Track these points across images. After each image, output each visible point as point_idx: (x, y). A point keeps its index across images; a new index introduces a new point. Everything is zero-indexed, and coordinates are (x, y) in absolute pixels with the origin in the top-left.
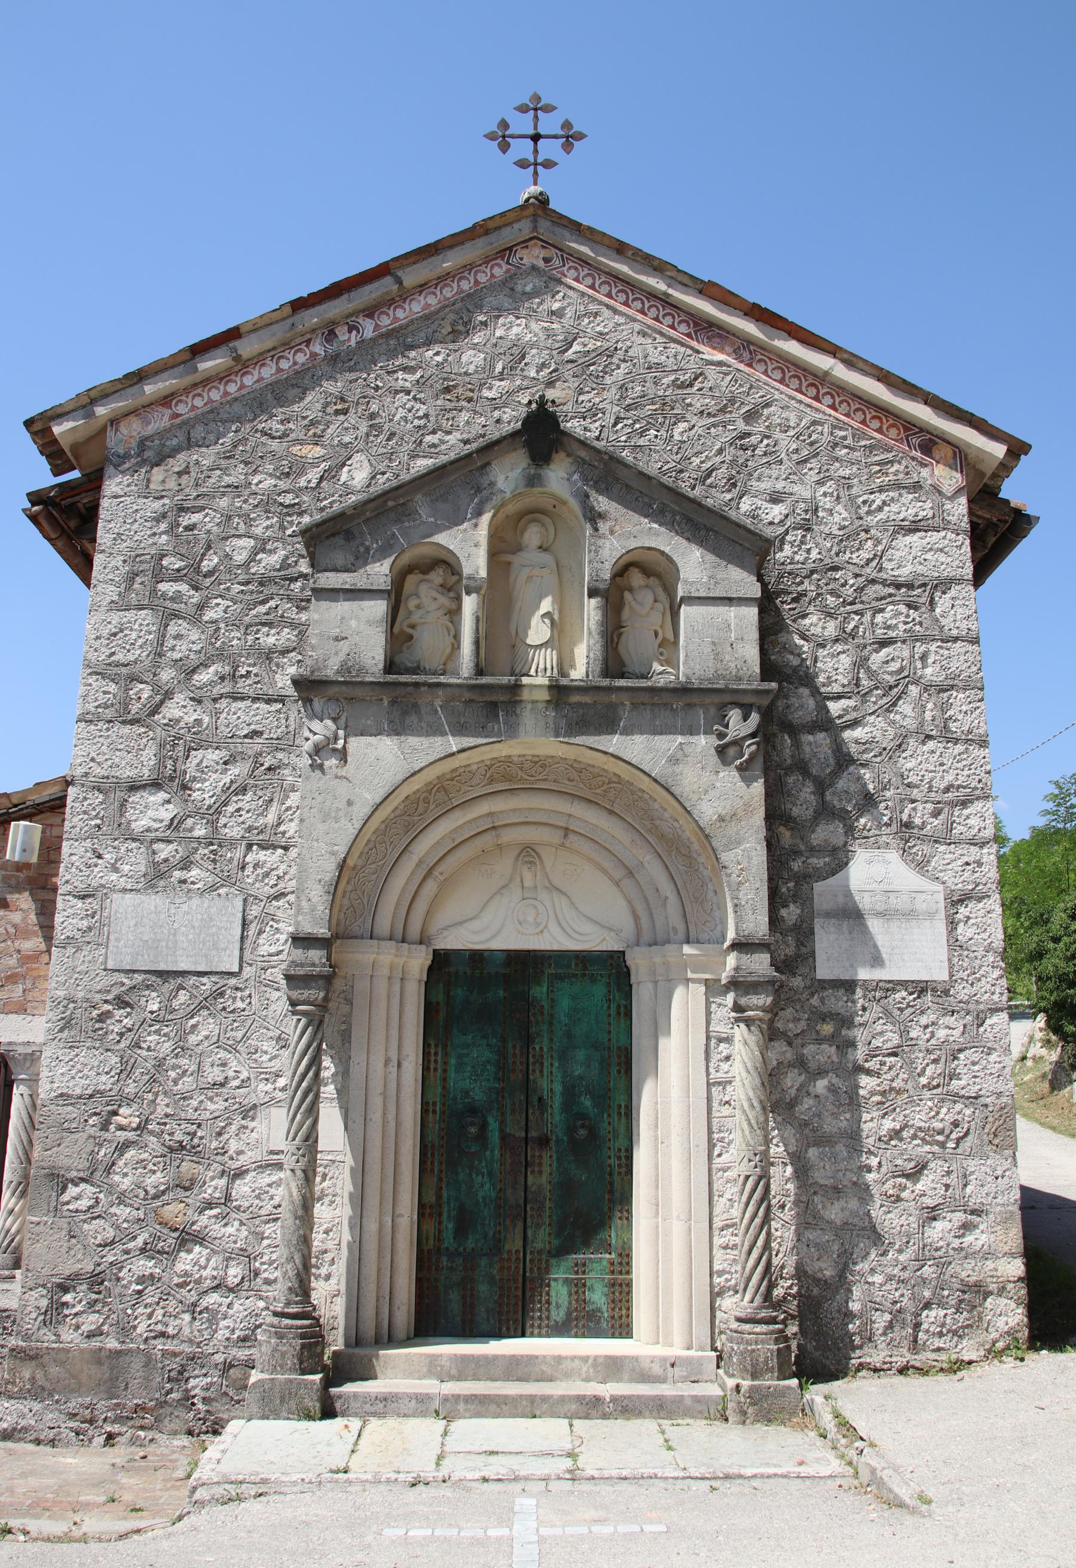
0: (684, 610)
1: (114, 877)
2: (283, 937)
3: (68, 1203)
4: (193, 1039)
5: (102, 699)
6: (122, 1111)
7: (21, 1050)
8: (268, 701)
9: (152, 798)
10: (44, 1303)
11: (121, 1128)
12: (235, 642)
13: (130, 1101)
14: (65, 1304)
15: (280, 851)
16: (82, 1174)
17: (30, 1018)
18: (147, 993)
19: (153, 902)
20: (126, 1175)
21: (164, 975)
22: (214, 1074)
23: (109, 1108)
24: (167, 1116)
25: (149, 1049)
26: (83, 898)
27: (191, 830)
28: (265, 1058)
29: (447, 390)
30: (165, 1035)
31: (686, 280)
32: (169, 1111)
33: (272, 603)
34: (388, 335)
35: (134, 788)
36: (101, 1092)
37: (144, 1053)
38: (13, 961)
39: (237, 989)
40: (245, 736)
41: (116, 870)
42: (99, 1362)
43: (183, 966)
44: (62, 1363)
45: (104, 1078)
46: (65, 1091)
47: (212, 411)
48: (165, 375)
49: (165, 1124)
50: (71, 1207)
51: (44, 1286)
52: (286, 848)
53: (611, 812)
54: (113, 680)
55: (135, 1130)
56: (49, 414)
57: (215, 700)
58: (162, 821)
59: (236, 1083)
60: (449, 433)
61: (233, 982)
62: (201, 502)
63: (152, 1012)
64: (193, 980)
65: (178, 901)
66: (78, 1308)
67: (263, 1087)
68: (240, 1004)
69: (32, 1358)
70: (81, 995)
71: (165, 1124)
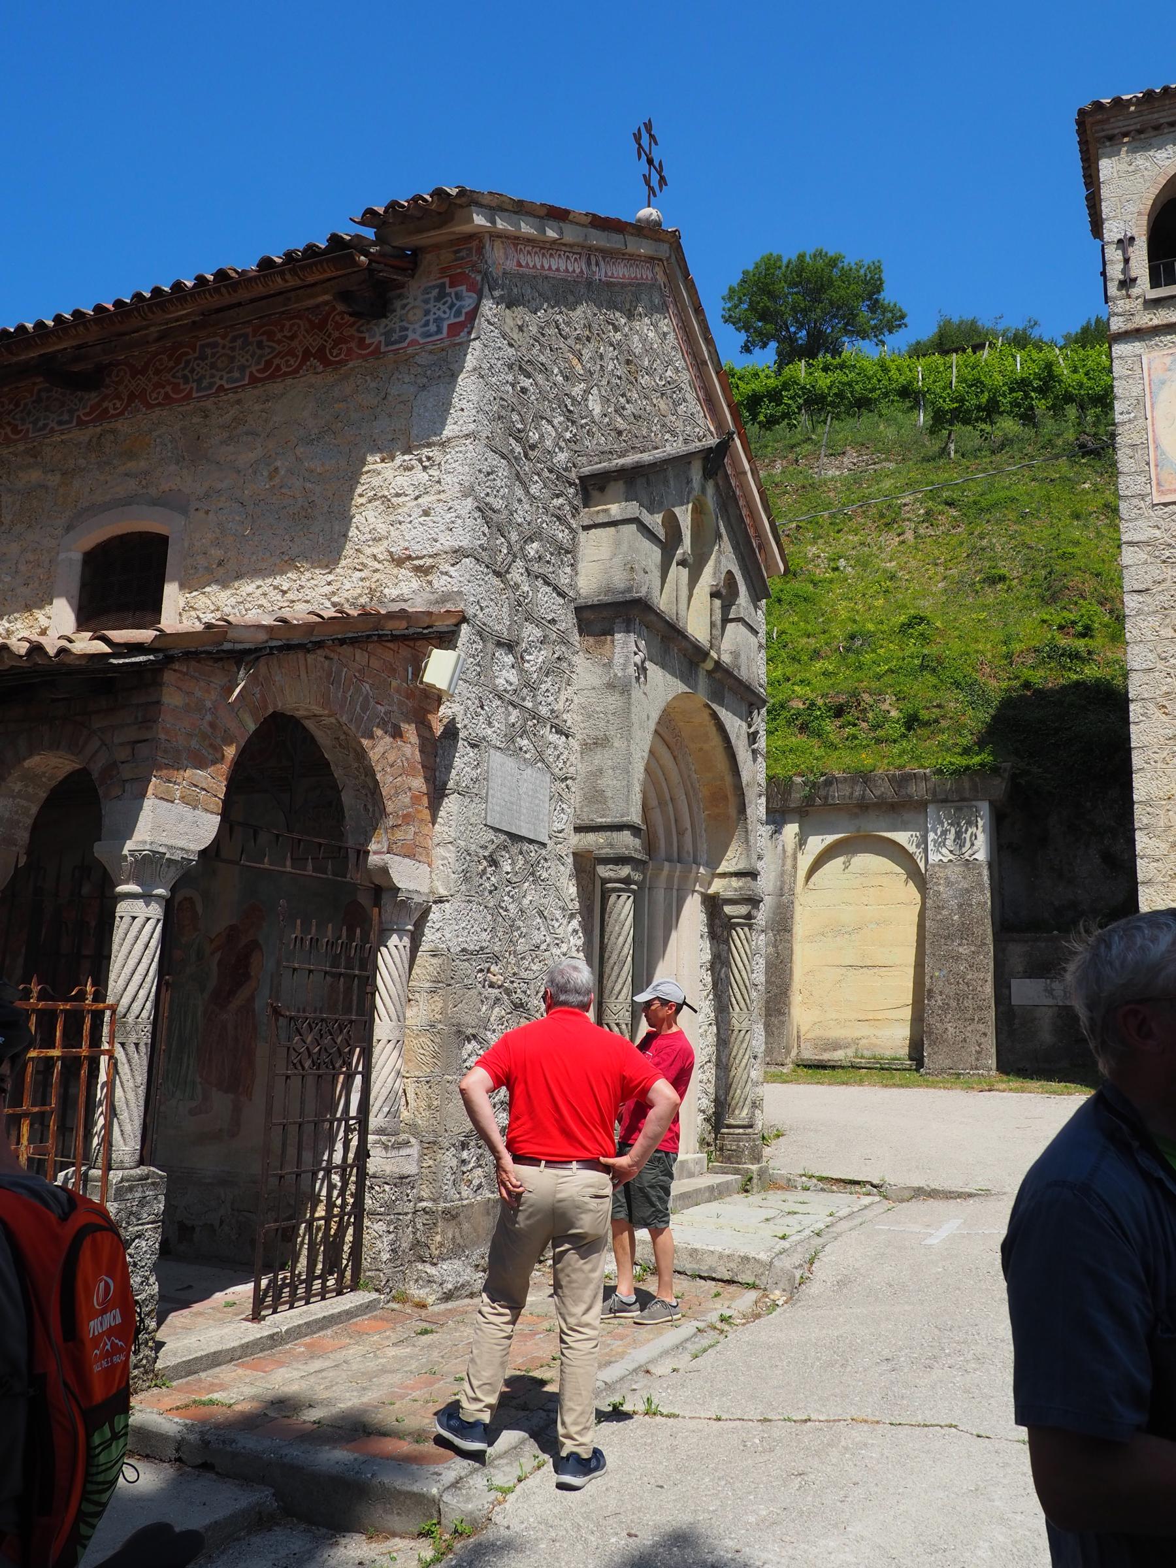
0: (730, 627)
1: (489, 731)
2: (565, 817)
3: (465, 1061)
4: (526, 902)
5: (483, 541)
6: (493, 968)
7: (417, 899)
8: (559, 594)
9: (506, 659)
10: (454, 1162)
11: (492, 985)
12: (544, 525)
13: (496, 959)
14: (464, 1162)
15: (564, 738)
16: (474, 1031)
17: (417, 864)
18: (503, 853)
19: (510, 763)
20: (494, 1031)
21: (515, 838)
22: (537, 937)
23: (487, 965)
24: (514, 974)
25: (506, 910)
26: (473, 746)
27: (524, 699)
28: (557, 925)
29: (628, 362)
30: (512, 897)
31: (715, 360)
32: (516, 970)
33: (561, 500)
34: (609, 285)
35: (499, 644)
36: (482, 948)
37: (504, 913)
38: (407, 800)
39: (546, 860)
40: (549, 622)
41: (490, 724)
42: (488, 1214)
43: (523, 833)
44: (468, 1218)
45: (484, 934)
46: (466, 946)
47: (534, 277)
48: (531, 219)
49: (512, 982)
50: (467, 1064)
51: (454, 1145)
52: (567, 737)
53: (675, 758)
54: (487, 523)
55: (499, 987)
56: (475, 195)
57: (537, 577)
58: (511, 684)
59: (543, 947)
60: (628, 402)
61: (544, 852)
62: (529, 369)
63: (507, 873)
64: (526, 847)
65: (522, 767)
66: (472, 1165)
67: (555, 951)
68: (545, 875)
69: (454, 1217)
70: (473, 847)
71: (512, 982)
